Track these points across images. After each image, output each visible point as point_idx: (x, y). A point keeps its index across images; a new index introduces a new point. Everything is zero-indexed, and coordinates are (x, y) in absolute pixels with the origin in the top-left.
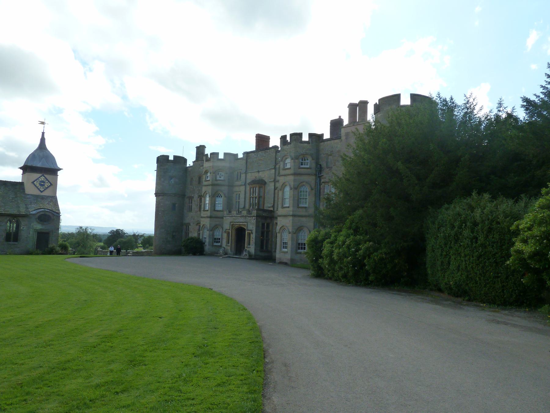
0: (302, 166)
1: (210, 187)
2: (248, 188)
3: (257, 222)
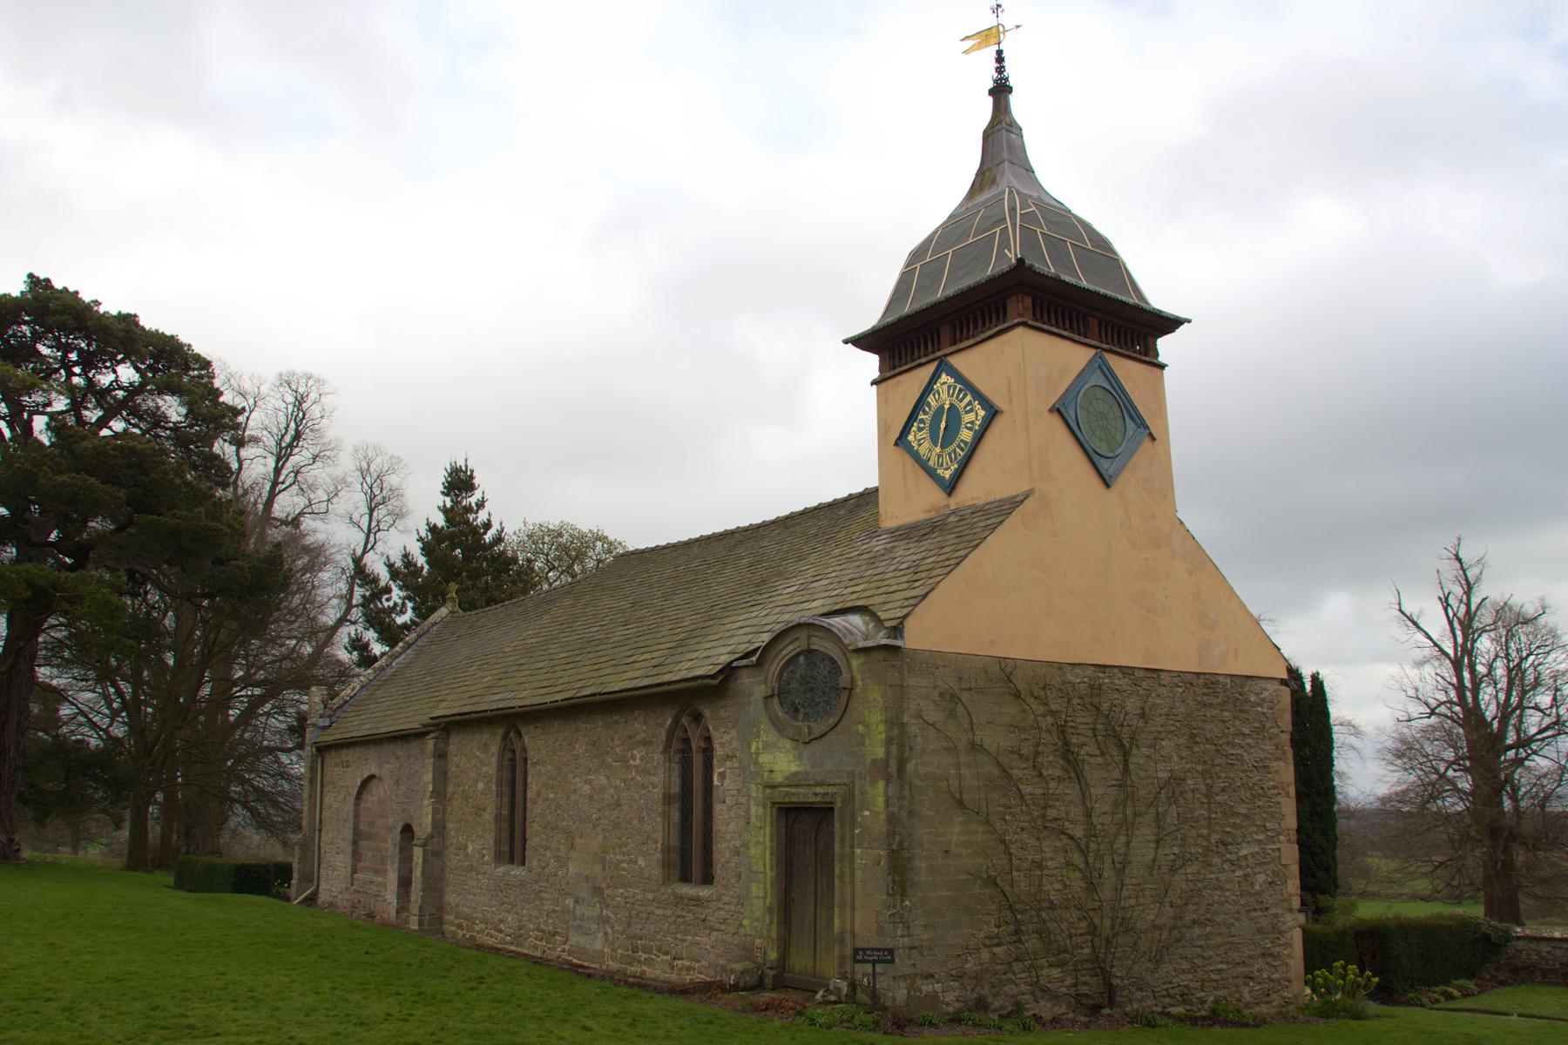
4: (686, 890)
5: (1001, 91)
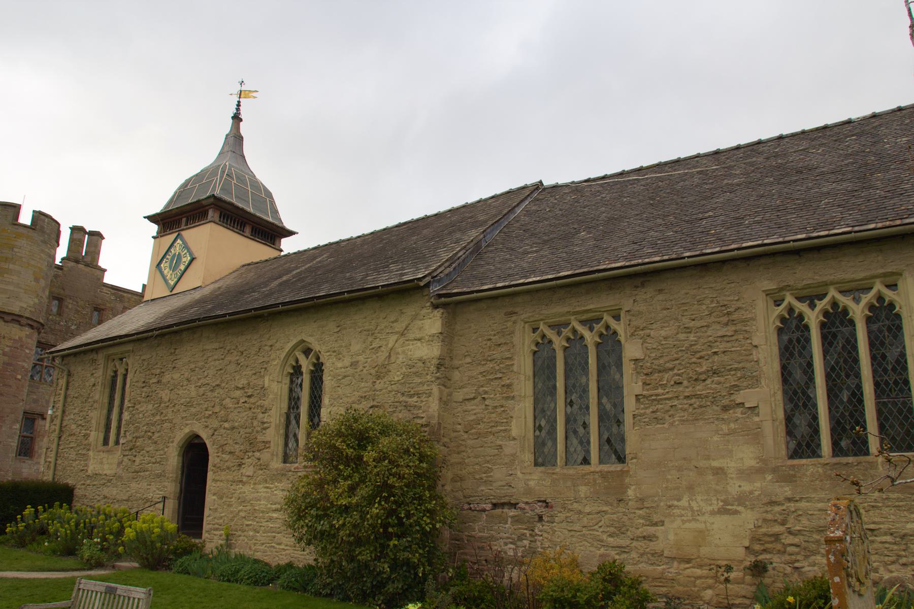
5: (237, 118)
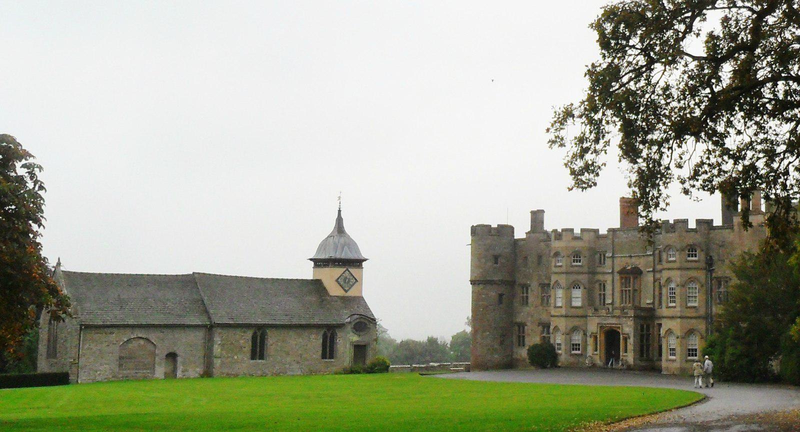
0: (691, 258)
1: (564, 276)
2: (617, 277)
3: (635, 323)
4: (326, 360)
5: (340, 211)
